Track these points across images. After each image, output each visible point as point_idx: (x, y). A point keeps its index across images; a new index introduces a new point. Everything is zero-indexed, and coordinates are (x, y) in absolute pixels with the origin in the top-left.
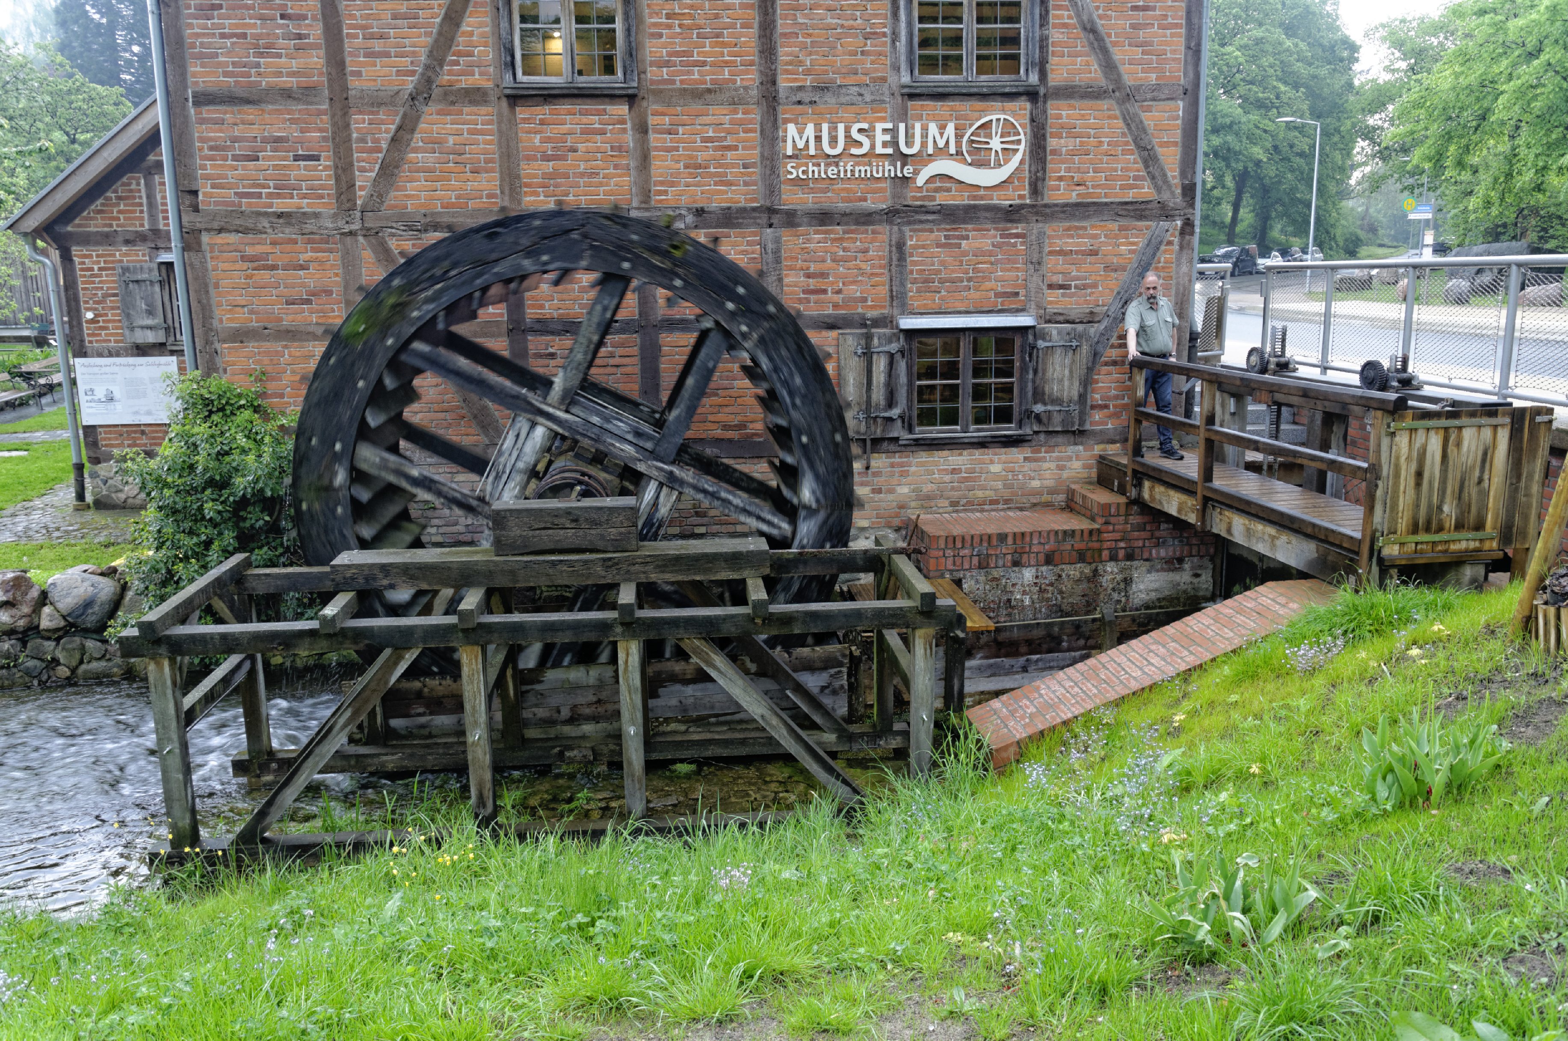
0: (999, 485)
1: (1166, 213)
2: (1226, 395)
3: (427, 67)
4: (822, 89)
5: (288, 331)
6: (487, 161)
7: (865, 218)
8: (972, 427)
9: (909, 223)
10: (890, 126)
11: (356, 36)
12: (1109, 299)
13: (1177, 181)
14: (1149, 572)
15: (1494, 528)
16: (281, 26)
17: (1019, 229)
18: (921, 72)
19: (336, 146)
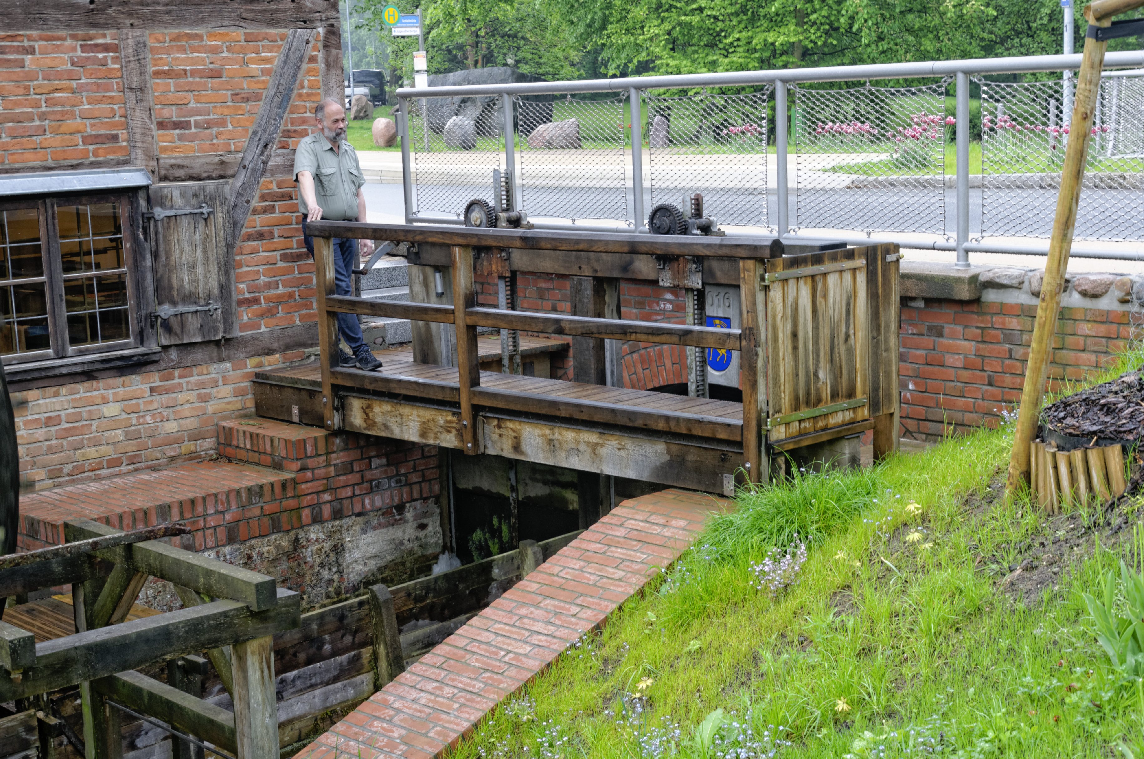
2: (429, 270)
12: (243, 142)
14: (364, 531)
15: (864, 393)
17: (108, 38)
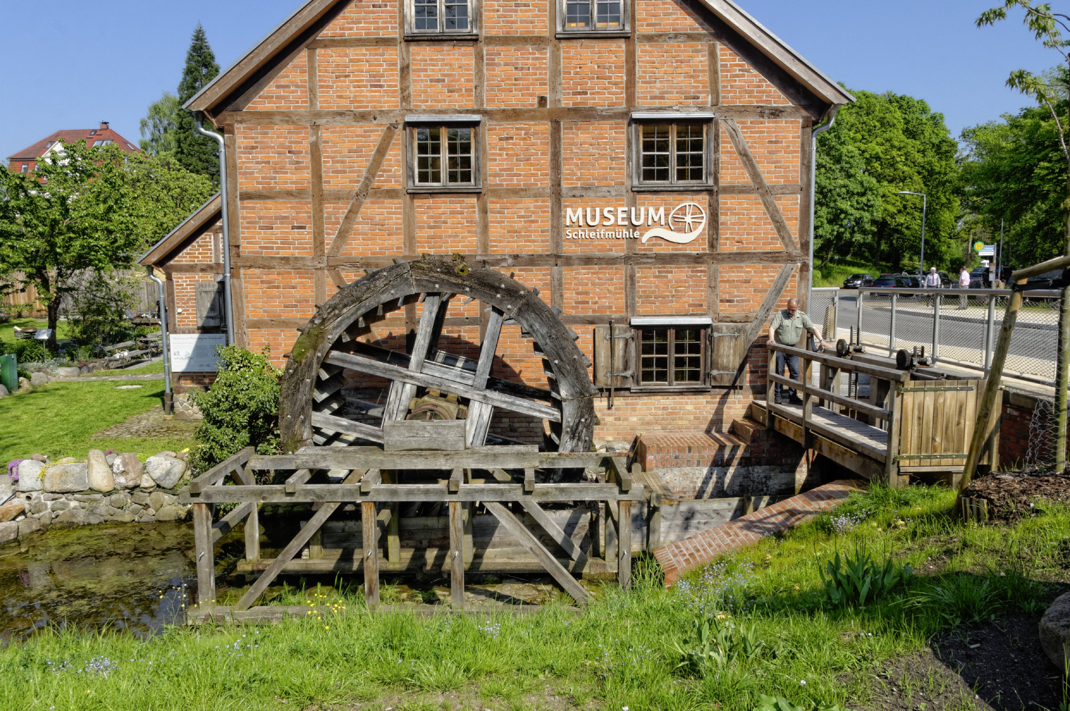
0: (692, 417)
1: (791, 259)
3: (367, 178)
4: (586, 189)
5: (284, 322)
6: (397, 229)
7: (612, 261)
8: (675, 383)
9: (638, 264)
10: (626, 209)
11: (328, 162)
12: (758, 309)
13: (798, 240)
14: (781, 472)
16: (288, 157)
18: (644, 179)
19: (315, 221)
